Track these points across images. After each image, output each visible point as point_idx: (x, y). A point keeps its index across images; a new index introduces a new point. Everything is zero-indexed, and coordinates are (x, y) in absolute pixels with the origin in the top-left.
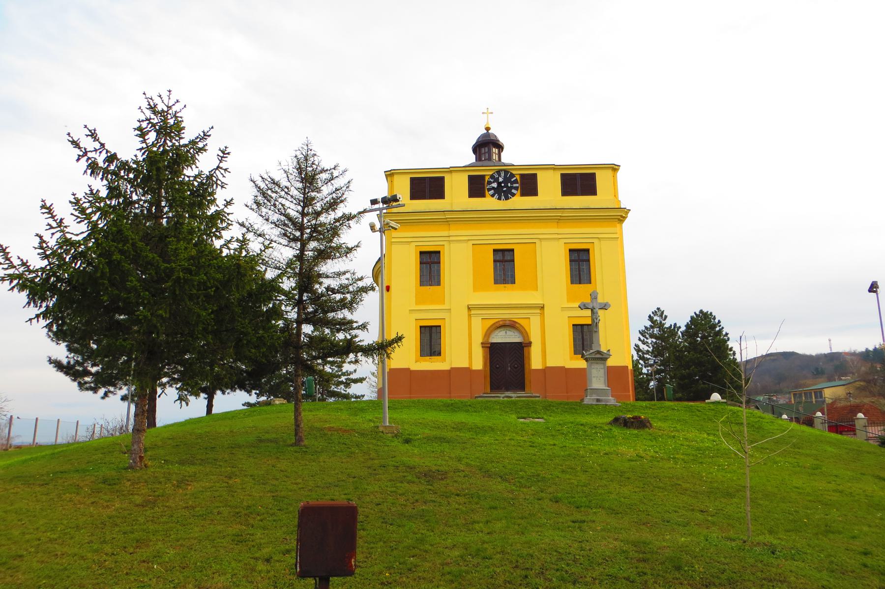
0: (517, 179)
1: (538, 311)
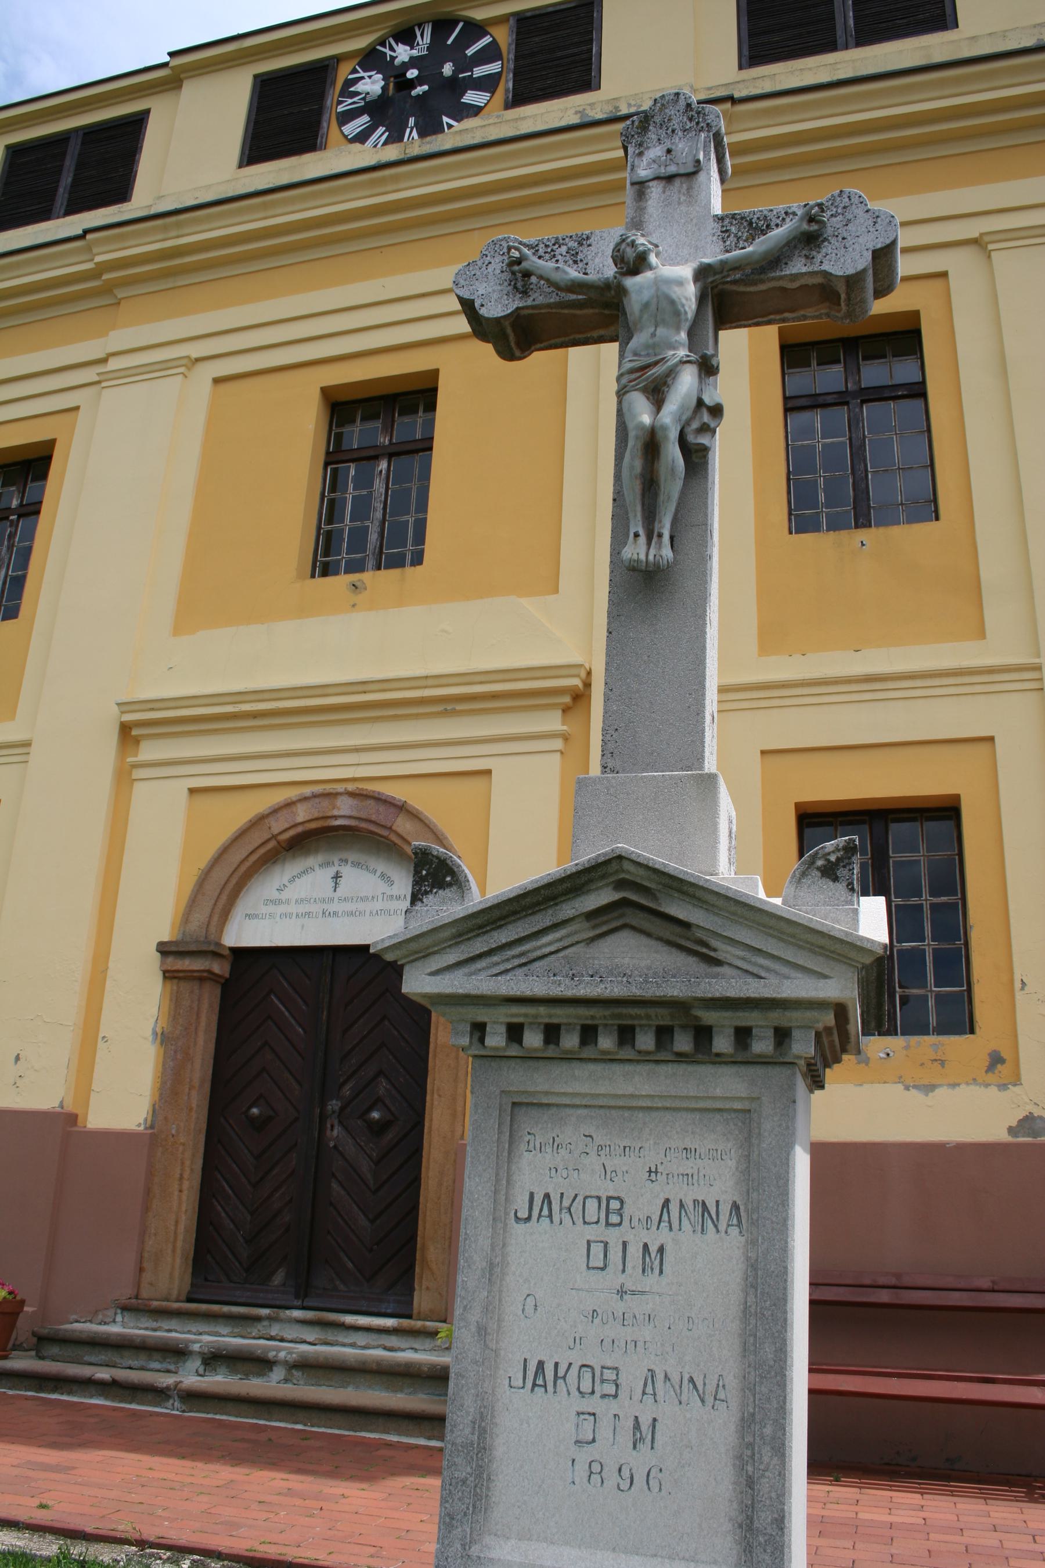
0: (494, 44)
1: (553, 722)
